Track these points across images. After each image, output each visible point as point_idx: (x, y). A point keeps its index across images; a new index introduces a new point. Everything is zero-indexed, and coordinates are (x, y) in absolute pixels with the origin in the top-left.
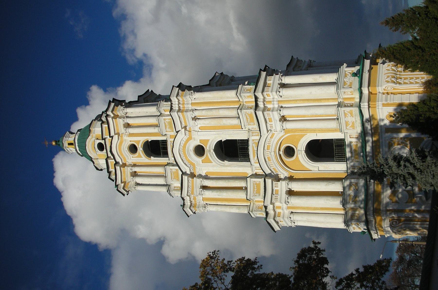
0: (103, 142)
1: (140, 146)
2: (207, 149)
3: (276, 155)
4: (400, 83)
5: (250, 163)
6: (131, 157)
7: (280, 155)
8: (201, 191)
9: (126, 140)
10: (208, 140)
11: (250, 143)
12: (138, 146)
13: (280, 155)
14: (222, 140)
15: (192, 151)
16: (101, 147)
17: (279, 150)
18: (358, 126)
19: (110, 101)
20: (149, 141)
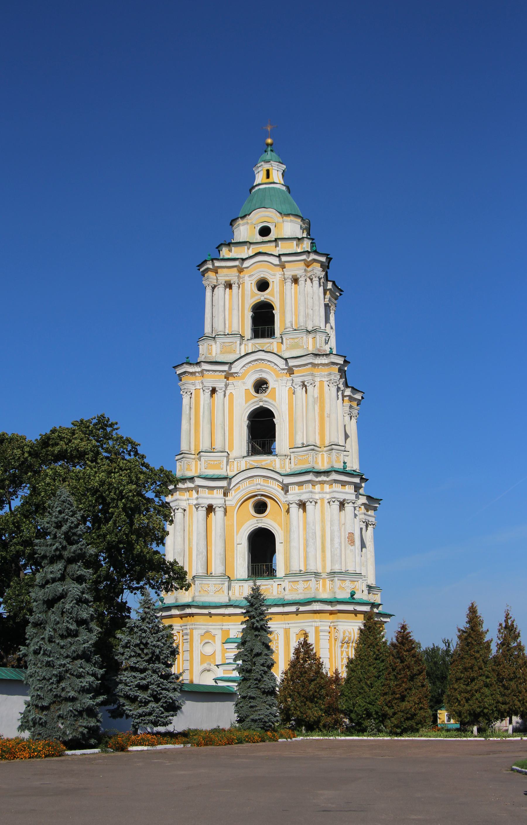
0: (272, 236)
1: (266, 296)
2: (263, 396)
3: (257, 490)
4: (342, 647)
5: (245, 454)
6: (251, 282)
7: (256, 496)
8: (209, 389)
9: (274, 275)
10: (275, 400)
11: (270, 458)
12: (267, 294)
13: (256, 496)
14: (274, 417)
15: (261, 376)
16: (265, 231)
17: (262, 495)
18: (292, 596)
19: (328, 255)
20: (274, 311)
